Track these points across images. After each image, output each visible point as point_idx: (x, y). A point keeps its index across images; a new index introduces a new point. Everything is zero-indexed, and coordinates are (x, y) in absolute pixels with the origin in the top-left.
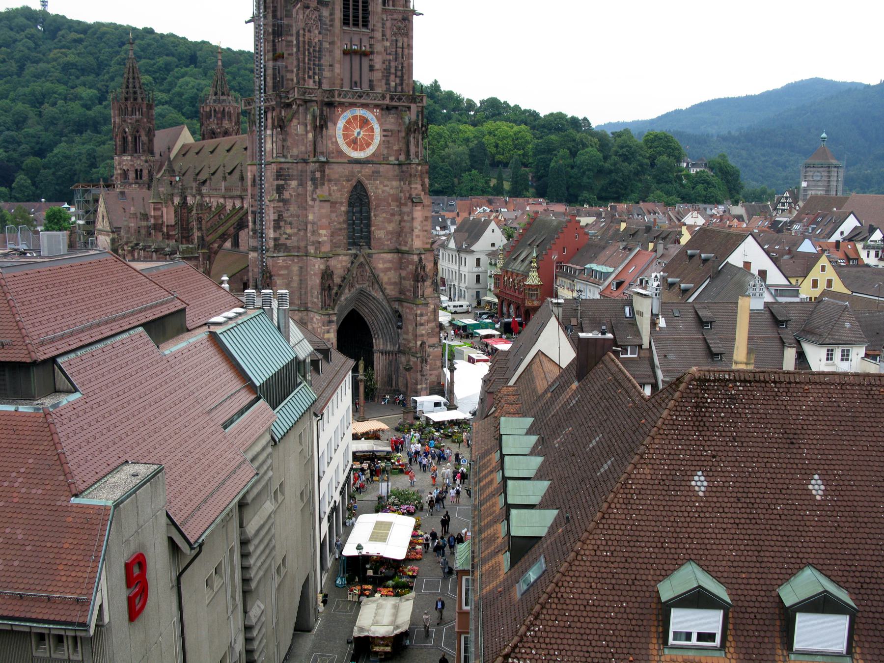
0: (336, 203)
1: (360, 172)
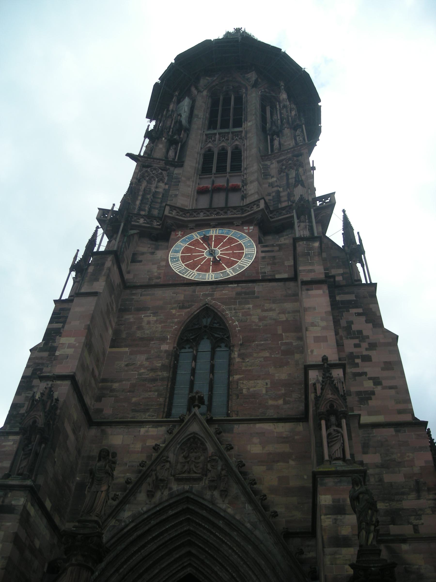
0: (151, 339)
1: (206, 295)
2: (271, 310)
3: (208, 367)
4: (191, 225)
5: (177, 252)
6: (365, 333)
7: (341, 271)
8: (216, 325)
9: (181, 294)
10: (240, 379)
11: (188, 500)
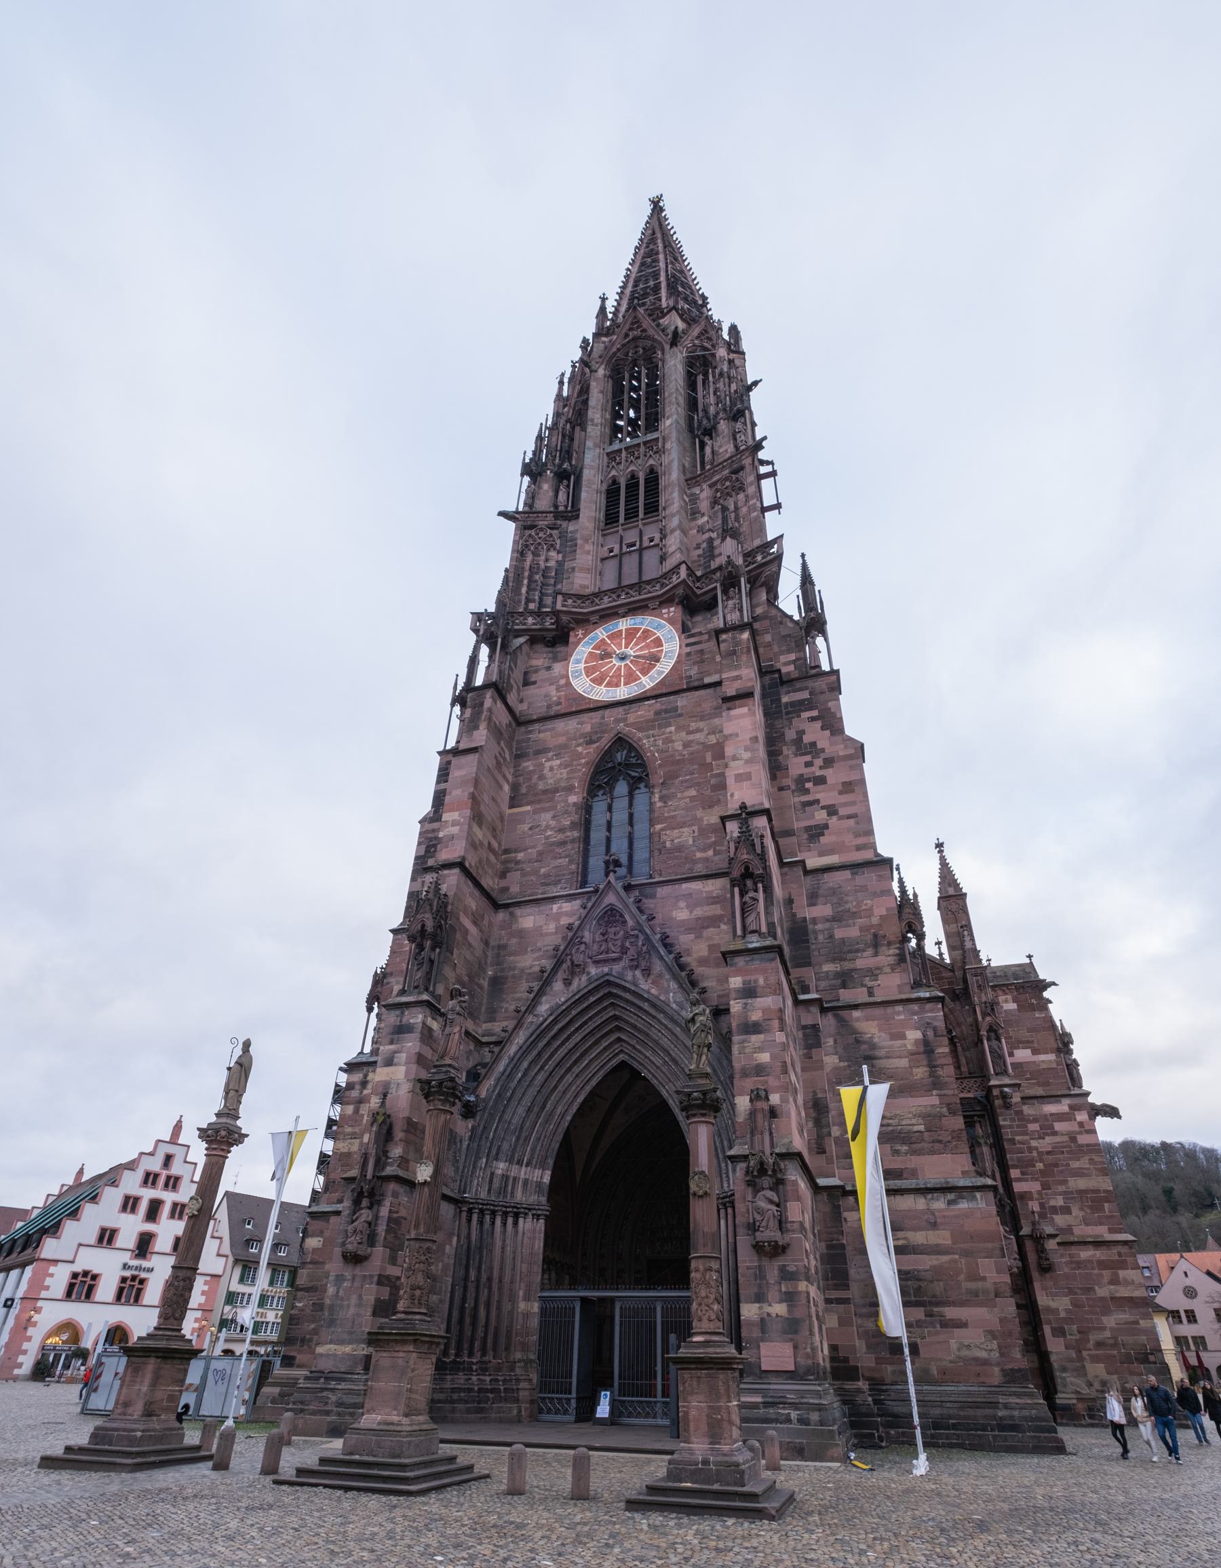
0: (556, 790)
1: (617, 721)
2: (698, 730)
3: (626, 816)
4: (594, 618)
5: (578, 661)
6: (819, 746)
7: (793, 657)
8: (633, 761)
9: (587, 724)
10: (662, 830)
11: (609, 983)
